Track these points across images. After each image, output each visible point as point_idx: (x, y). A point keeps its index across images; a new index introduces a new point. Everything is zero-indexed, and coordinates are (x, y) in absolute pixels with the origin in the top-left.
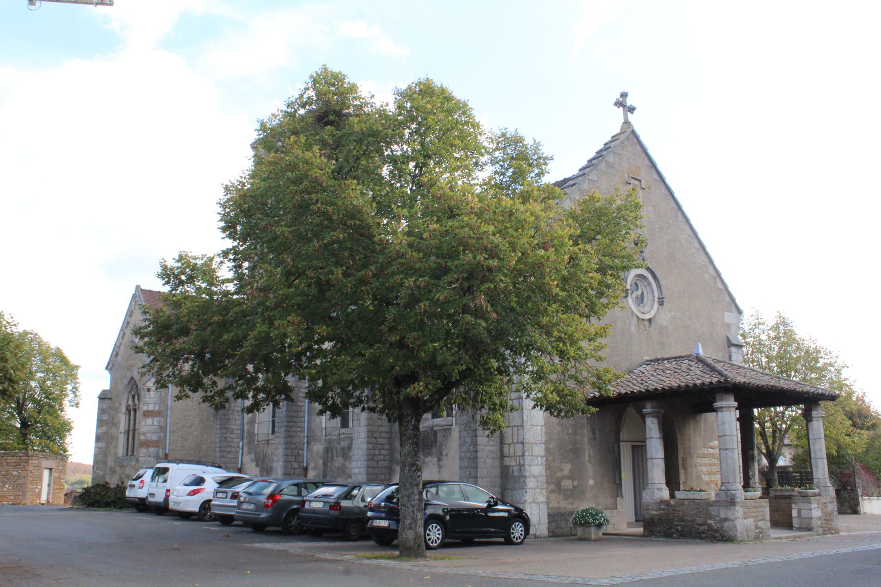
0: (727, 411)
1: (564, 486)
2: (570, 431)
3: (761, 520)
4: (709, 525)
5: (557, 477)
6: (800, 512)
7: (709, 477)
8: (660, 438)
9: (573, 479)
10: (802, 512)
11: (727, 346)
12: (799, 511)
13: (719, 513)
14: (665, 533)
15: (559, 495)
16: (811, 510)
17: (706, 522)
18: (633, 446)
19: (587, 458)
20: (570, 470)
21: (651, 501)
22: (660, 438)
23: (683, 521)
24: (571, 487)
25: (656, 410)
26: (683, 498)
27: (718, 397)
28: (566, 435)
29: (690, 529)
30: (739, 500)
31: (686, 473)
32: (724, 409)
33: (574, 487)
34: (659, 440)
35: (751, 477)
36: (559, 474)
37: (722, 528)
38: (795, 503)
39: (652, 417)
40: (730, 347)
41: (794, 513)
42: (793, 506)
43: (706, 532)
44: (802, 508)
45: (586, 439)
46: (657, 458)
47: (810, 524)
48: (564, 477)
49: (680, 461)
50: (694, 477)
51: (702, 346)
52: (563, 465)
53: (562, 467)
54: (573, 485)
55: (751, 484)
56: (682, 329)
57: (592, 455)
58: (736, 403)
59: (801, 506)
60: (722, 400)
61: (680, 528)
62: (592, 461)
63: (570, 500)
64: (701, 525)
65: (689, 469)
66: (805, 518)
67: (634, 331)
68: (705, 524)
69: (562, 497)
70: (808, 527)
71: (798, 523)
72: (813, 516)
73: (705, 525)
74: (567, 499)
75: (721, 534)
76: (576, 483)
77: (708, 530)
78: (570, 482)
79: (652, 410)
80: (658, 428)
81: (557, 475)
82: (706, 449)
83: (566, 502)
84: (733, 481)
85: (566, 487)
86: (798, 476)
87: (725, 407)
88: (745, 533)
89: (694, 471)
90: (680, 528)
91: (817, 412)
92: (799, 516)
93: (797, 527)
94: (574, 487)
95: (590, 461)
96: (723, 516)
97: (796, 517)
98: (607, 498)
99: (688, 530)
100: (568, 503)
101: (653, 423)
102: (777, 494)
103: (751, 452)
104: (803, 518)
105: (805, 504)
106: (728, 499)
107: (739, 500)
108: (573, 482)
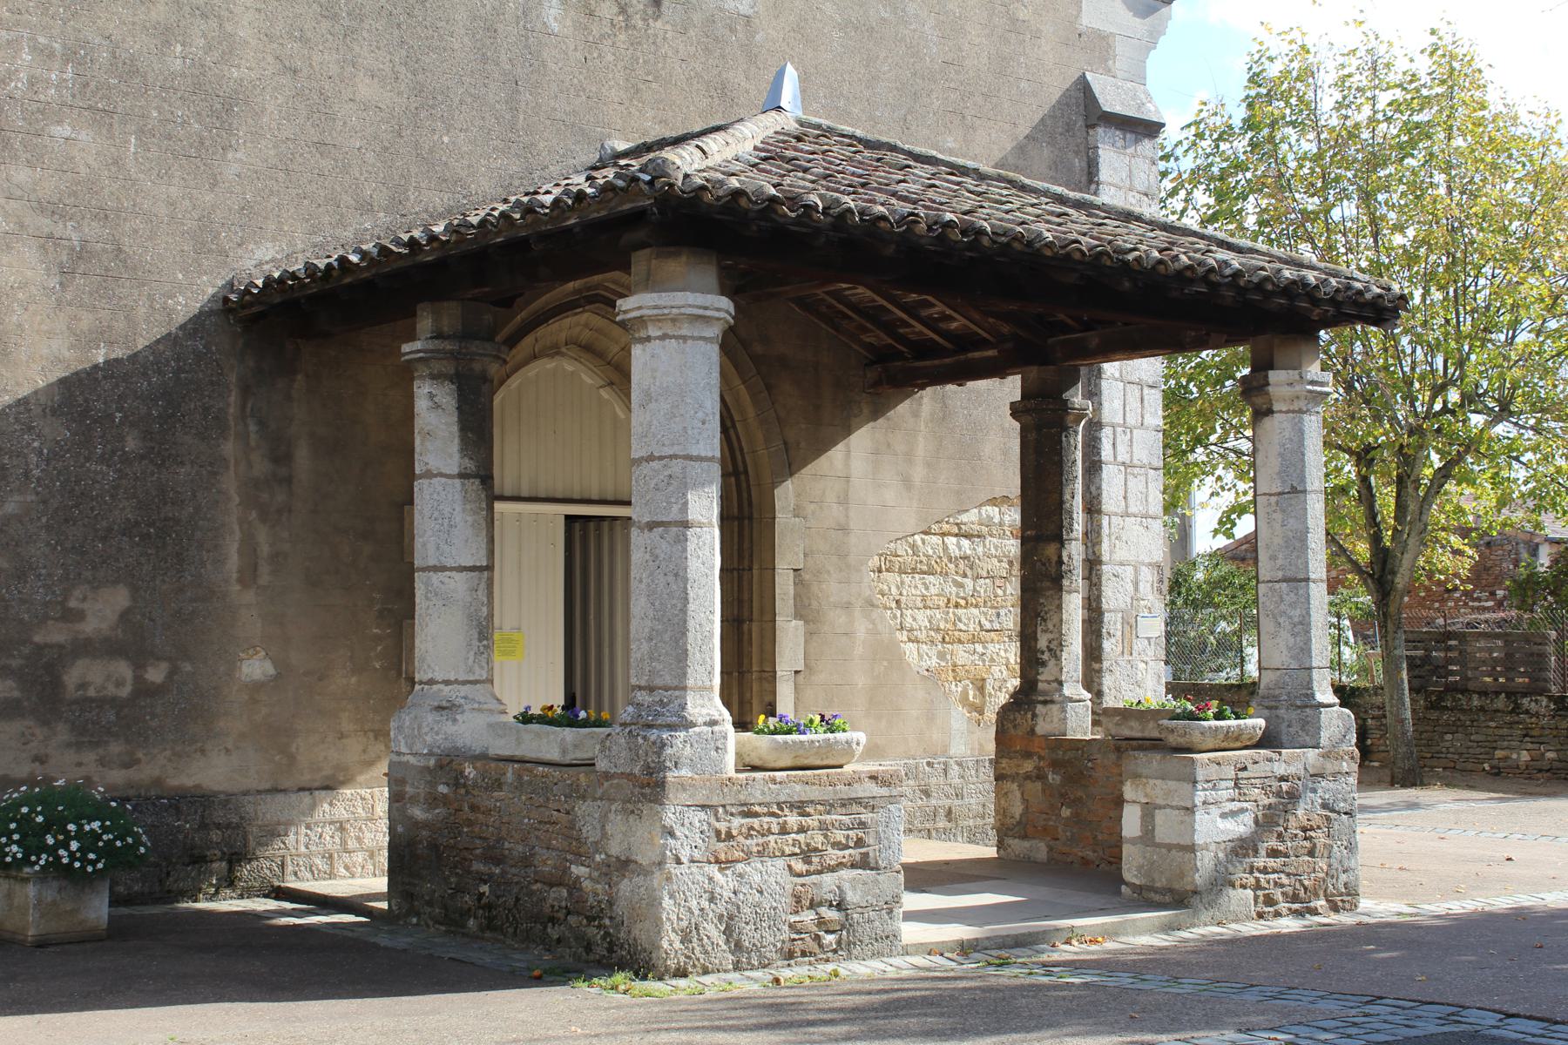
0: (664, 337)
1: (83, 686)
2: (132, 444)
3: (832, 869)
4: (574, 886)
5: (40, 648)
6: (1153, 817)
7: (941, 656)
8: (462, 476)
9: (139, 656)
10: (1160, 817)
11: (1080, 123)
12: (1149, 811)
13: (604, 835)
14: (445, 907)
15: (45, 723)
16: (1190, 810)
17: (566, 871)
18: (570, 519)
19: (233, 561)
20: (124, 616)
21: (412, 760)
22: (462, 476)
23: (498, 861)
24: (125, 692)
25: (448, 346)
26: (507, 753)
27: (641, 261)
28: (102, 459)
29: (518, 899)
30: (685, 772)
31: (810, 635)
32: (653, 331)
33: (144, 690)
34: (457, 482)
35: (1046, 657)
36: (55, 634)
37: (611, 903)
38: (1136, 776)
39: (433, 377)
40: (1093, 126)
41: (1131, 822)
42: (1129, 791)
43: (561, 915)
44: (1160, 801)
45: (230, 483)
46: (443, 569)
47: (1182, 875)
48: (85, 648)
49: (784, 585)
50: (859, 650)
51: (804, 80)
52: (77, 593)
53: (73, 604)
54: (138, 679)
55: (1041, 686)
56: (836, 34)
57: (265, 549)
58: (725, 303)
59: (1157, 789)
60: (649, 284)
61: (485, 889)
62: (264, 579)
63: (116, 748)
64: (551, 885)
65: (838, 619)
66: (1169, 847)
67: (555, 27)
68: (560, 879)
69: (63, 733)
70: (1176, 886)
71: (1139, 868)
72: (1199, 839)
73: (560, 884)
74: (95, 745)
75: (607, 934)
76: (156, 674)
77: (569, 913)
78: (124, 669)
79: (437, 345)
80: (455, 428)
81: (37, 639)
82: (935, 540)
83: (90, 757)
84: (668, 680)
85: (91, 693)
86: (1498, 649)
87: (657, 320)
88: (713, 931)
89: (861, 628)
90: (485, 889)
91: (1293, 374)
92: (1148, 836)
93: (1138, 882)
94: (144, 690)
95: (249, 575)
96: (615, 848)
97: (1133, 841)
98: (342, 736)
99: (511, 902)
100: (102, 762)
101: (437, 406)
102: (1127, 733)
103: (1051, 550)
104: (1159, 845)
105: (1172, 784)
106: (636, 771)
107: (685, 772)
108: (139, 667)
